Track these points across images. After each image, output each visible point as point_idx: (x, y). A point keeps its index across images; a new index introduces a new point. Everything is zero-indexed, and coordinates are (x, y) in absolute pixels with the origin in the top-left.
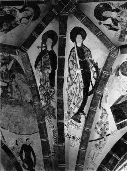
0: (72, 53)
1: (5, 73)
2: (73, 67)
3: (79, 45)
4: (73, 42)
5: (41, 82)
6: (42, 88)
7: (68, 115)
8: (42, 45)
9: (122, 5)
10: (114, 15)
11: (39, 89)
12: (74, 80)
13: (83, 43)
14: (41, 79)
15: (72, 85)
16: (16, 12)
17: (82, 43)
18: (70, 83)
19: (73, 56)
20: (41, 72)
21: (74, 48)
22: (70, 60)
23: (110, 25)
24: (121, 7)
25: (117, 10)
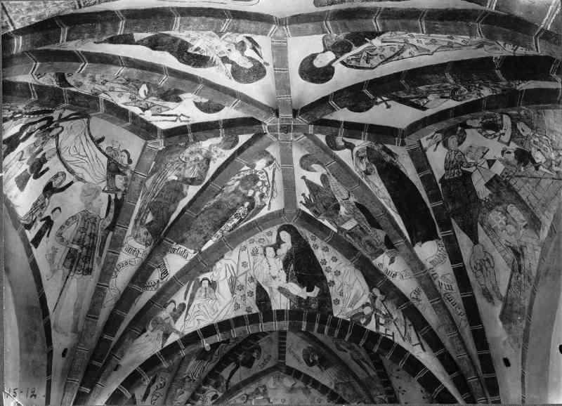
0: (353, 63)
1: (483, 119)
2: (376, 55)
3: (330, 56)
4: (333, 68)
5: (447, 98)
6: (457, 93)
7: (485, 46)
8: (381, 102)
9: (213, 66)
10: (235, 56)
11: (461, 100)
12: (402, 45)
13: (322, 50)
14: (442, 97)
15: (416, 47)
16: (358, 151)
17: (324, 52)
18: (413, 49)
19: (358, 60)
20: (429, 98)
21: (343, 63)
22: (369, 66)
23: (254, 49)
24: (217, 63)
25: (225, 60)
